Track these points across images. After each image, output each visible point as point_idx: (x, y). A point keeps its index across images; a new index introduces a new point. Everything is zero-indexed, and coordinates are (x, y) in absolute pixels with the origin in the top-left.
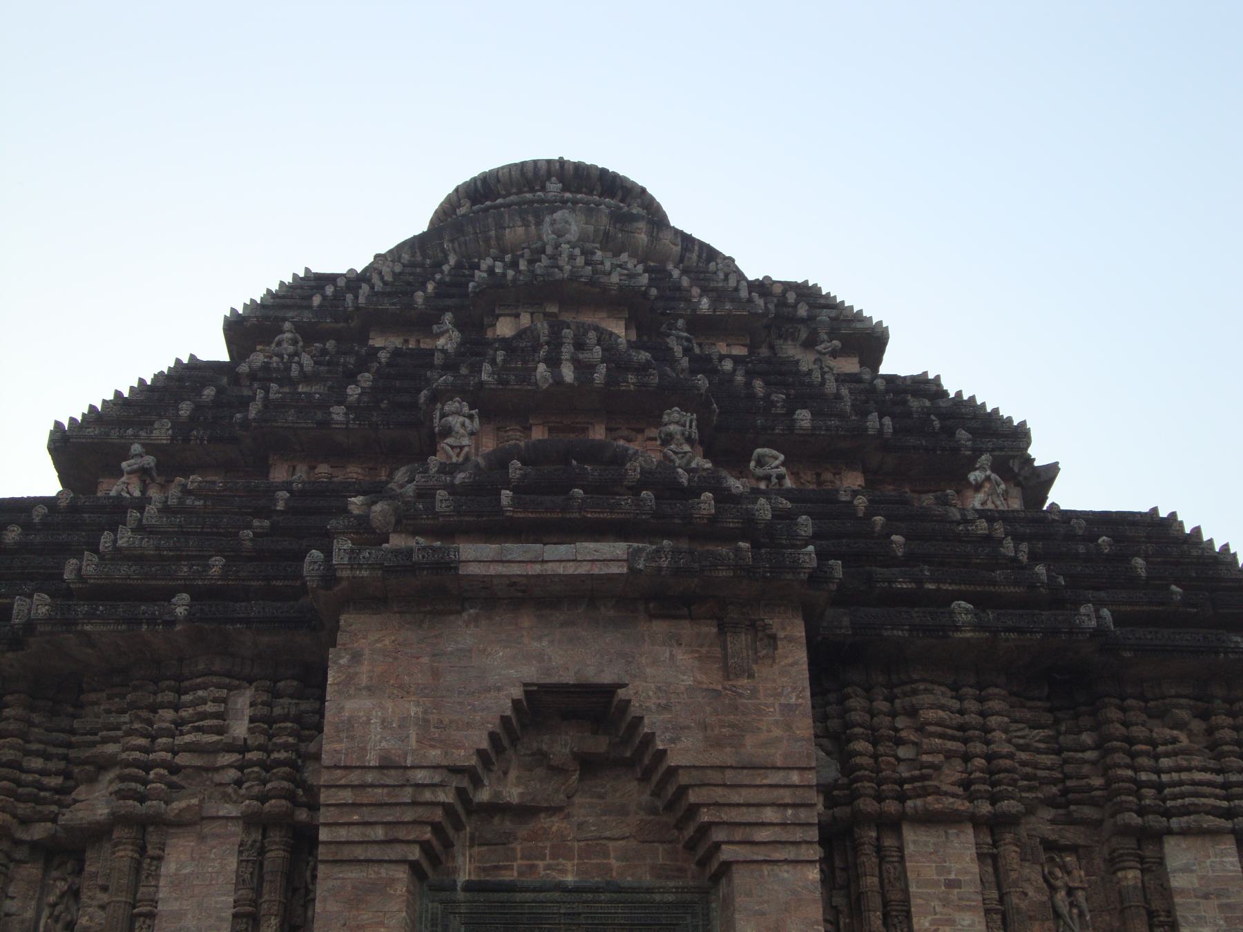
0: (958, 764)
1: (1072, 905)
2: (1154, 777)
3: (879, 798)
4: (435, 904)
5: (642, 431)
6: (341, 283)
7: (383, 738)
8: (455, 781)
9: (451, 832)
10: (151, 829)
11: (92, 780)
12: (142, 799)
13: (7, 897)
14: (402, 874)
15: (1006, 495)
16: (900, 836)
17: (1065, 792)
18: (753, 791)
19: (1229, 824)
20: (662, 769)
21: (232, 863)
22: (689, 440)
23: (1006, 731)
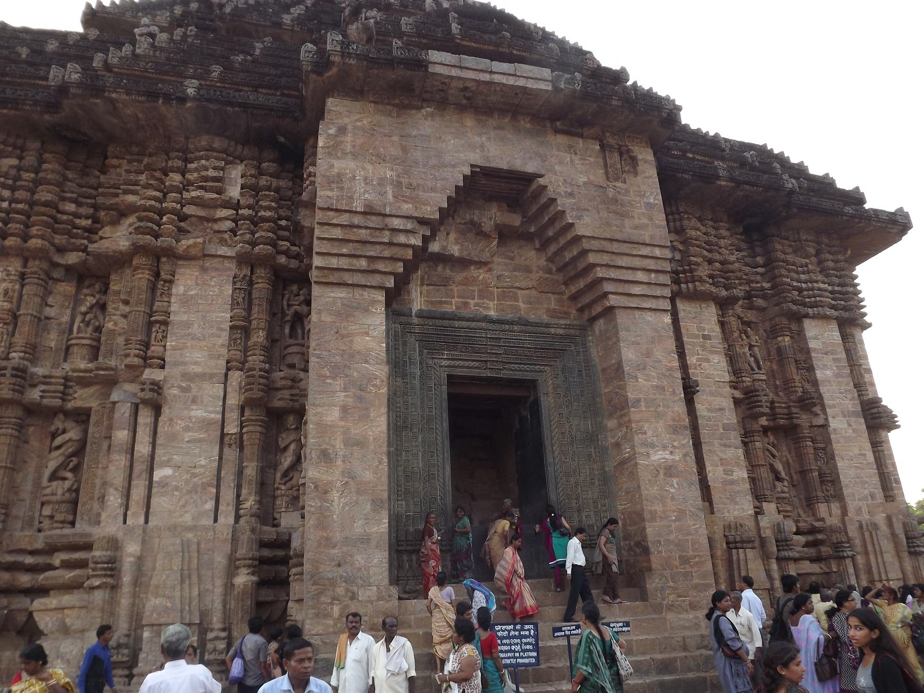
4: (397, 325)
7: (366, 192)
10: (164, 259)
11: (115, 223)
12: (157, 236)
13: (47, 305)
14: (381, 297)
18: (630, 259)
19: (835, 313)
20: (569, 236)
21: (228, 290)
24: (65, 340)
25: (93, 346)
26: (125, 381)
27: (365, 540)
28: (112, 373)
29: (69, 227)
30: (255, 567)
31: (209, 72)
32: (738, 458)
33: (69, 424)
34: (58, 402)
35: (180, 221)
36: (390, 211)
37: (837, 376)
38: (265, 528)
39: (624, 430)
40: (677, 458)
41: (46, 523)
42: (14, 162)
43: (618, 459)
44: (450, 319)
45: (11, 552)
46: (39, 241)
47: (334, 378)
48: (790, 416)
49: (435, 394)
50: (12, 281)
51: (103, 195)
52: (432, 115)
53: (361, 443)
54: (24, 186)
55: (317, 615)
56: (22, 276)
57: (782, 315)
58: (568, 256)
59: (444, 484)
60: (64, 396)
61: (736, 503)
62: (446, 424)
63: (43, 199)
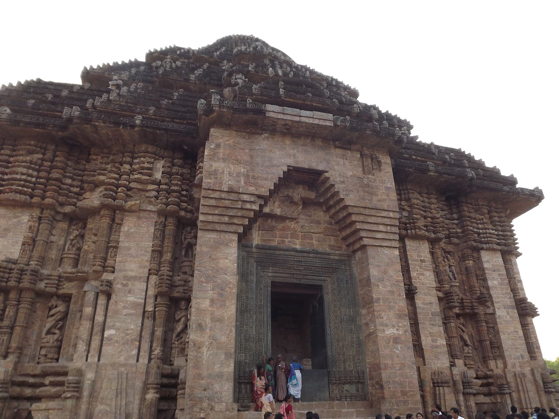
7: (229, 180)
10: (118, 212)
11: (92, 190)
12: (114, 199)
13: (52, 234)
14: (235, 238)
18: (375, 218)
19: (499, 248)
20: (342, 205)
21: (152, 230)
24: (60, 255)
25: (76, 259)
26: (92, 279)
27: (220, 376)
28: (85, 275)
29: (67, 192)
30: (158, 389)
31: (148, 110)
33: (60, 302)
34: (54, 290)
35: (128, 190)
36: (242, 191)
37: (501, 284)
38: (166, 366)
39: (371, 315)
40: (401, 333)
41: (42, 359)
42: (40, 156)
43: (367, 332)
44: (274, 250)
45: (21, 375)
46: (51, 200)
47: (207, 283)
48: (472, 308)
49: (264, 292)
51: (87, 175)
52: (267, 138)
53: (220, 320)
54: (45, 169)
56: (40, 218)
57: (468, 248)
58: (341, 216)
59: (267, 344)
60: (58, 287)
61: (439, 359)
62: (269, 310)
63: (54, 177)
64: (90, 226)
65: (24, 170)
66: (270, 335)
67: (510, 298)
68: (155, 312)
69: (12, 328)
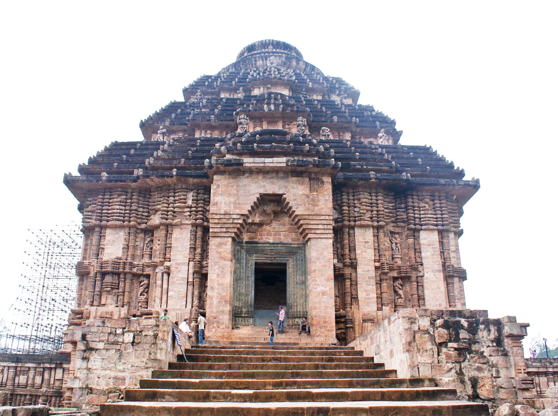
0: (370, 213)
1: (396, 247)
2: (419, 216)
3: (349, 221)
5: (292, 122)
6: (213, 78)
8: (243, 218)
9: (242, 229)
11: (155, 214)
12: (167, 219)
14: (230, 239)
15: (388, 140)
16: (354, 230)
17: (396, 219)
19: (436, 228)
21: (189, 235)
22: (304, 126)
23: (382, 204)
27: (223, 312)
32: (373, 289)
33: (145, 279)
34: (141, 272)
37: (432, 255)
40: (327, 289)
41: (140, 308)
42: (125, 197)
50: (127, 235)
55: (209, 331)
56: (129, 233)
60: (143, 270)
61: (369, 306)
64: (156, 235)
65: (118, 207)
66: (253, 292)
67: (439, 264)
68: (193, 282)
69: (124, 292)
